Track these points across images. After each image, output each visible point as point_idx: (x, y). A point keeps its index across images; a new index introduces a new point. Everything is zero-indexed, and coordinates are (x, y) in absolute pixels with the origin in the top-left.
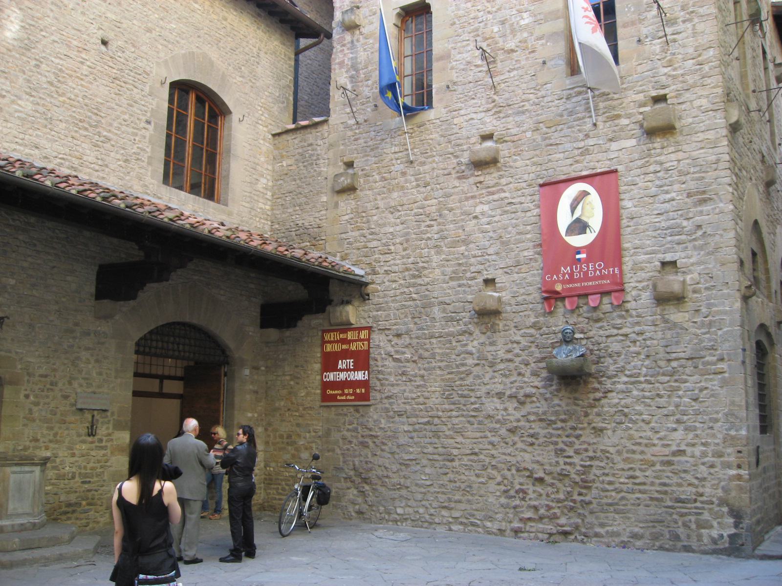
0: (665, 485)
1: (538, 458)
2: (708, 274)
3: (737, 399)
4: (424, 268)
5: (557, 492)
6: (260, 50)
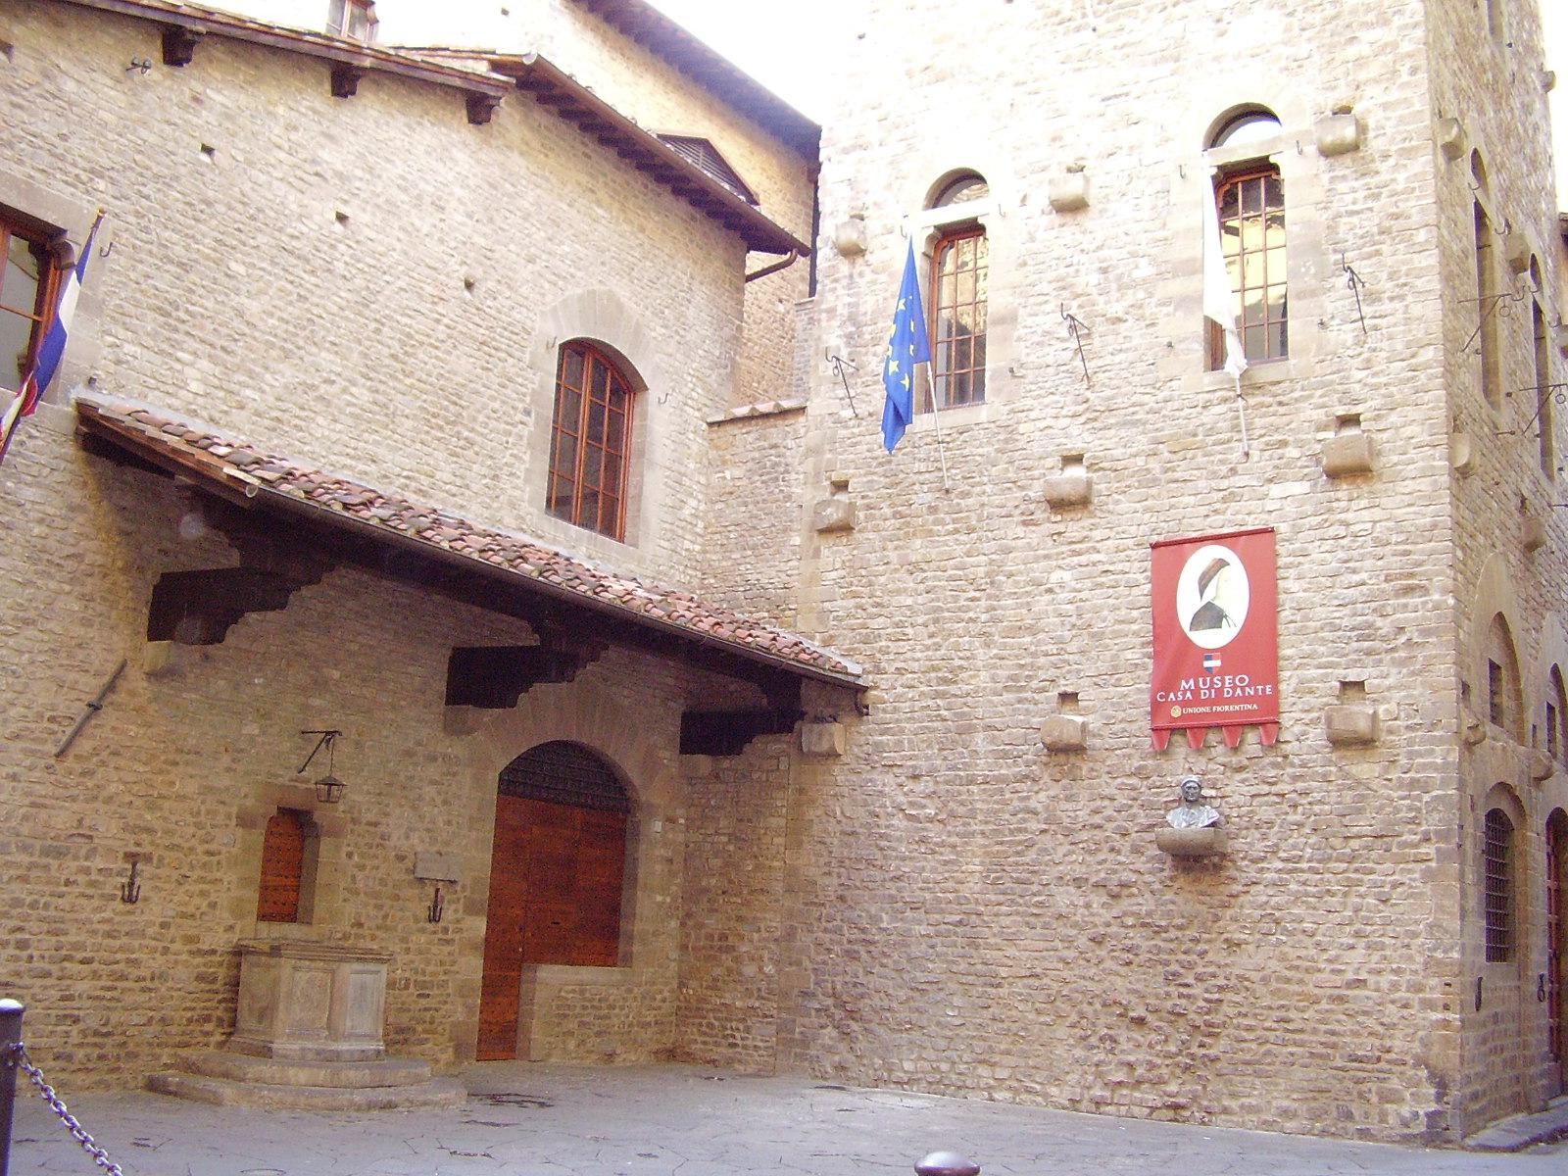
0: (1333, 1033)
1: (1139, 986)
3: (1446, 902)
4: (961, 667)
5: (1166, 1041)
6: (692, 278)
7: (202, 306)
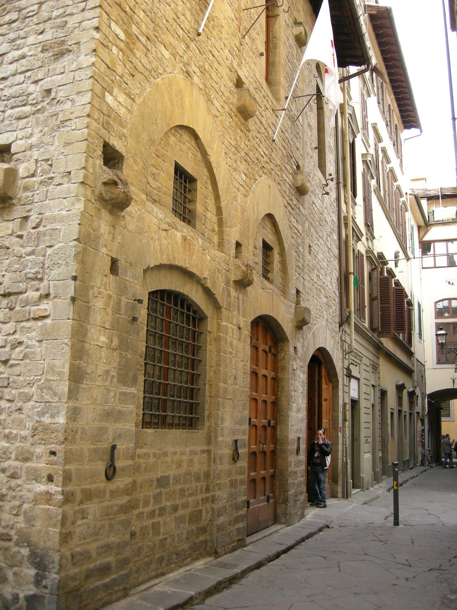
2: (48, 160)
3: (57, 363)
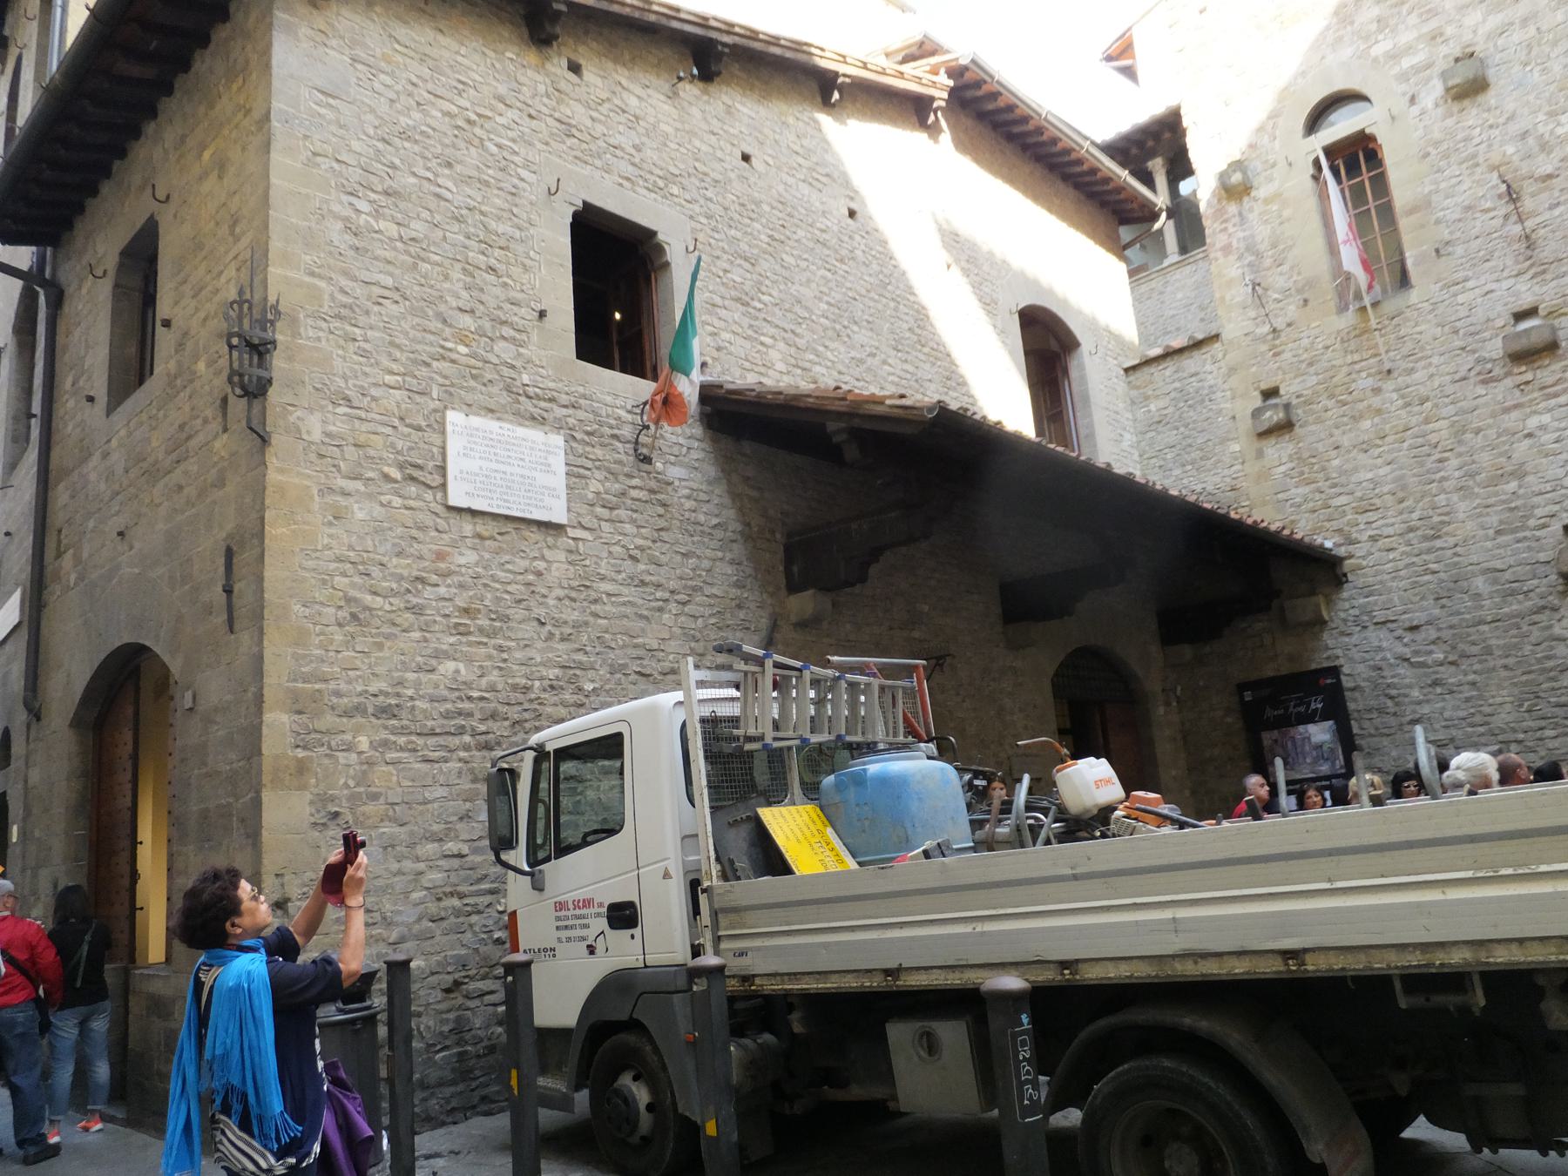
4: (1443, 523)
7: (770, 295)
